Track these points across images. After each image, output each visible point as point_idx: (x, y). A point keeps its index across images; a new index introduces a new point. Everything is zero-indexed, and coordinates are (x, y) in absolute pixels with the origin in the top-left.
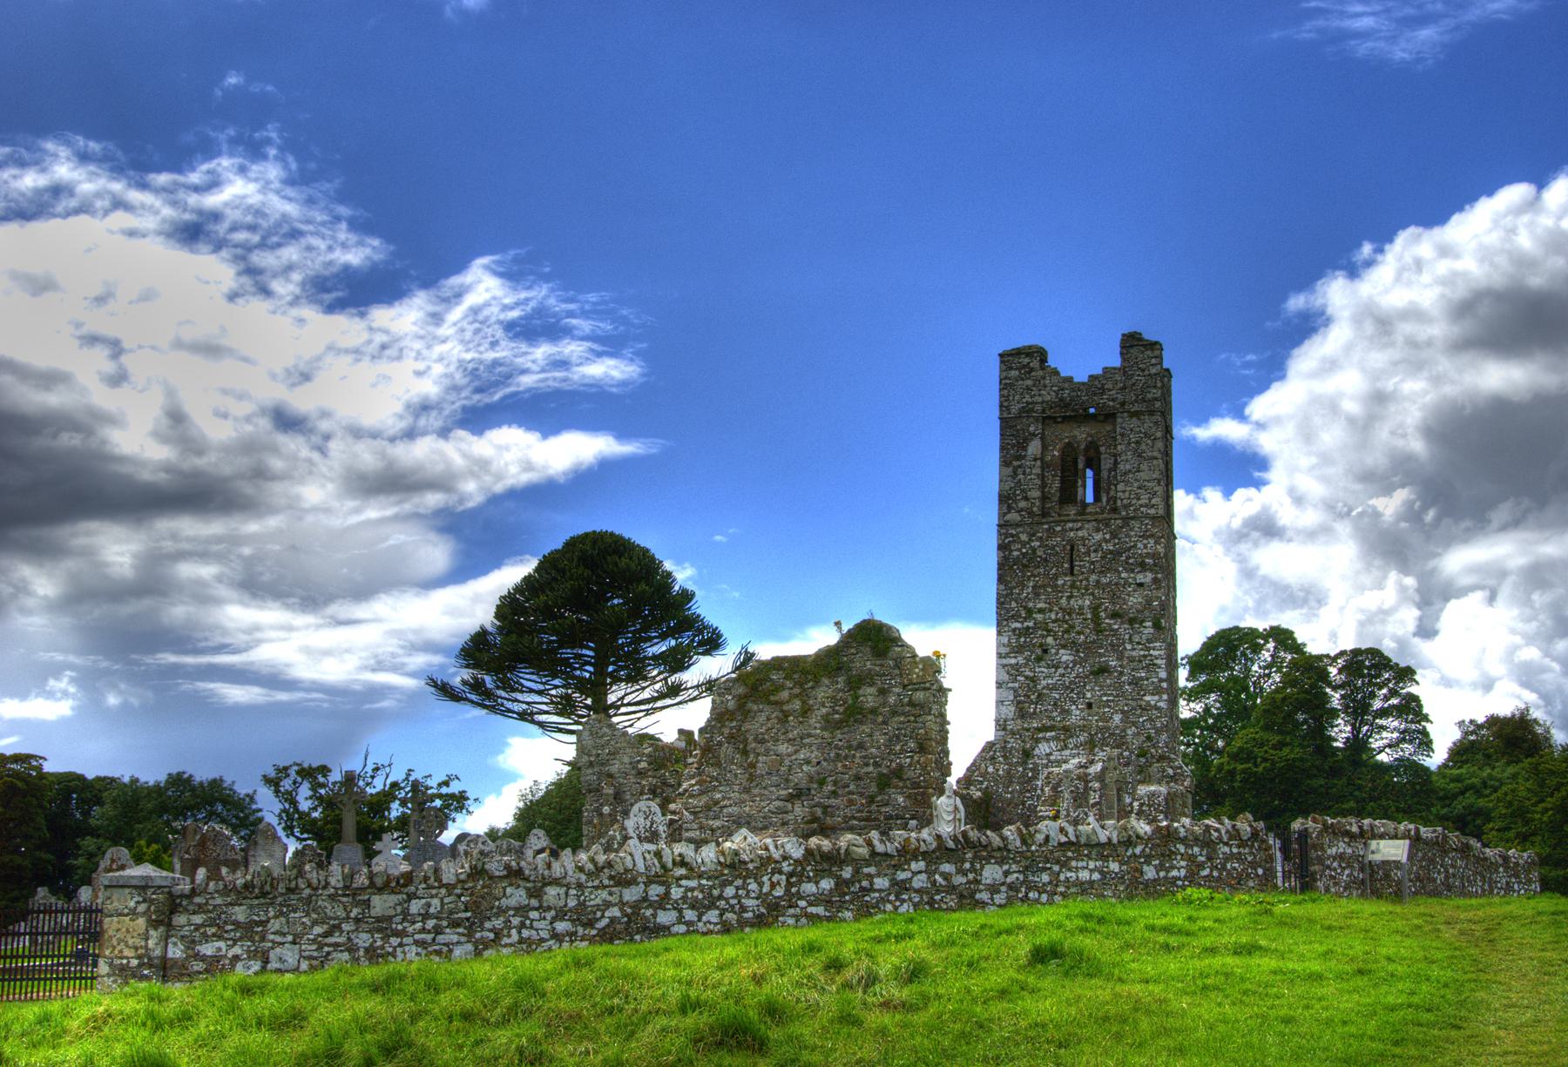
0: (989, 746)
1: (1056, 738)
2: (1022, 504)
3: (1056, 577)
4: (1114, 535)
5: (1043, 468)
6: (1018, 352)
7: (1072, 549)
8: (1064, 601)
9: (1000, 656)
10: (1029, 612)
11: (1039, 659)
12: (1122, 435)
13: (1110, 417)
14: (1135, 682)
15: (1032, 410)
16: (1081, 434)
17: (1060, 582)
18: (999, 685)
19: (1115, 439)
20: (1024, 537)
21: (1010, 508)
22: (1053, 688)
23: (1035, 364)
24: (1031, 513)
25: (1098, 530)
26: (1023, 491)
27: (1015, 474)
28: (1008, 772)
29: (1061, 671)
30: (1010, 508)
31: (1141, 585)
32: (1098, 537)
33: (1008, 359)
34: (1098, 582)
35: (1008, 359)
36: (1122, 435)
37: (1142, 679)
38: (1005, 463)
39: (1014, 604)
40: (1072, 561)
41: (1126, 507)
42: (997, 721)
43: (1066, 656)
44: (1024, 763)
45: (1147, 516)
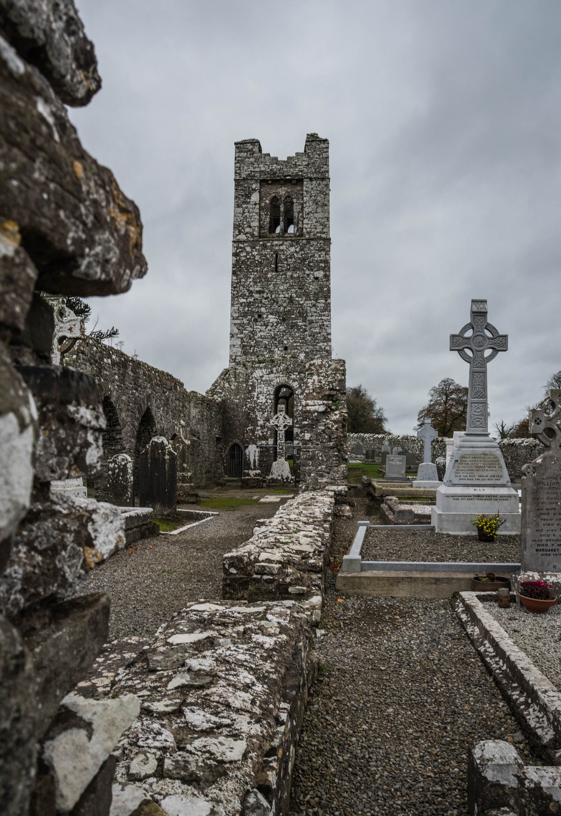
0: (226, 372)
1: (265, 367)
2: (248, 230)
3: (267, 273)
4: (302, 250)
6: (244, 143)
8: (271, 286)
9: (233, 318)
10: (251, 292)
11: (256, 320)
12: (307, 191)
13: (299, 181)
14: (312, 335)
15: (254, 176)
16: (282, 191)
17: (269, 275)
18: (232, 336)
19: (302, 194)
20: (248, 249)
21: (240, 232)
22: (265, 338)
23: (256, 149)
24: (253, 235)
25: (292, 246)
26: (248, 222)
27: (244, 213)
28: (237, 387)
29: (269, 328)
30: (240, 232)
31: (317, 278)
32: (292, 249)
33: (240, 146)
34: (292, 276)
35: (240, 146)
36: (307, 191)
37: (317, 333)
38: (238, 206)
40: (276, 264)
41: (309, 233)
42: (231, 356)
43: (272, 319)
44: (247, 381)
45: (320, 238)
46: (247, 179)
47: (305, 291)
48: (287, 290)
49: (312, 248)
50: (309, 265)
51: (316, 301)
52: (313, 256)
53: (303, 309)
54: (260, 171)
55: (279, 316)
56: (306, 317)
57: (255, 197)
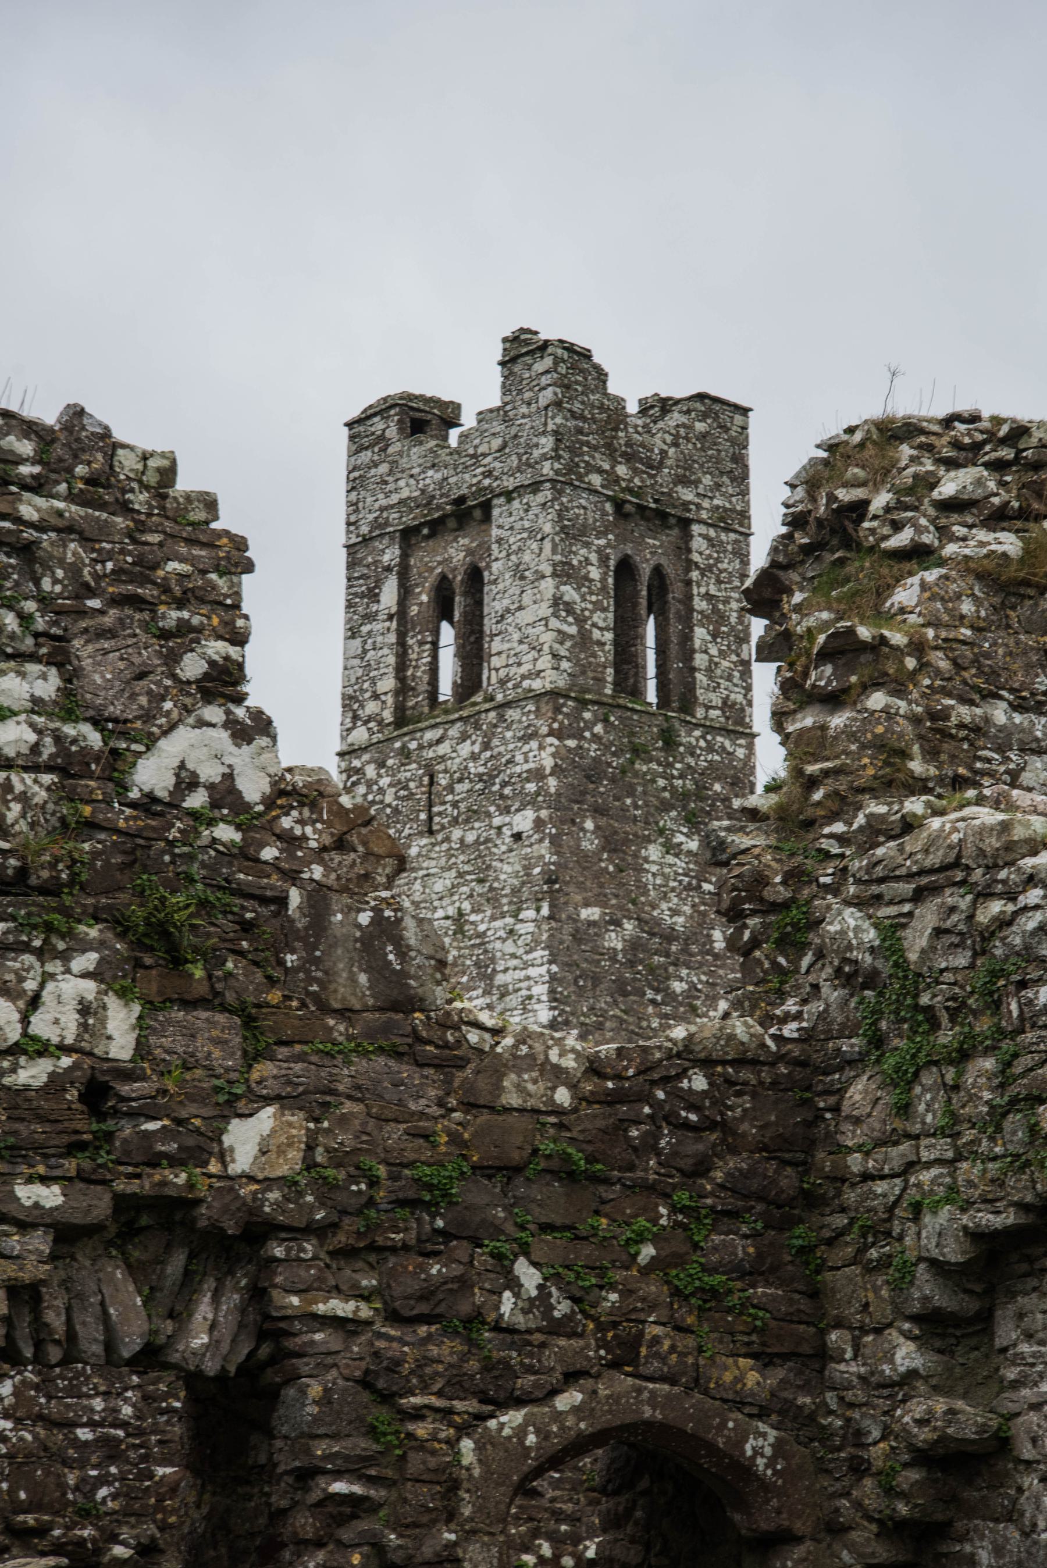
4: (486, 746)
5: (402, 636)
7: (431, 783)
12: (499, 541)
13: (486, 507)
15: (387, 523)
16: (455, 552)
20: (371, 771)
25: (464, 737)
30: (355, 718)
31: (517, 837)
32: (466, 749)
34: (462, 840)
38: (352, 633)
46: (371, 538)
47: (491, 889)
48: (452, 891)
49: (509, 734)
50: (502, 797)
51: (516, 916)
53: (486, 951)
54: (401, 502)
56: (491, 978)
57: (389, 595)
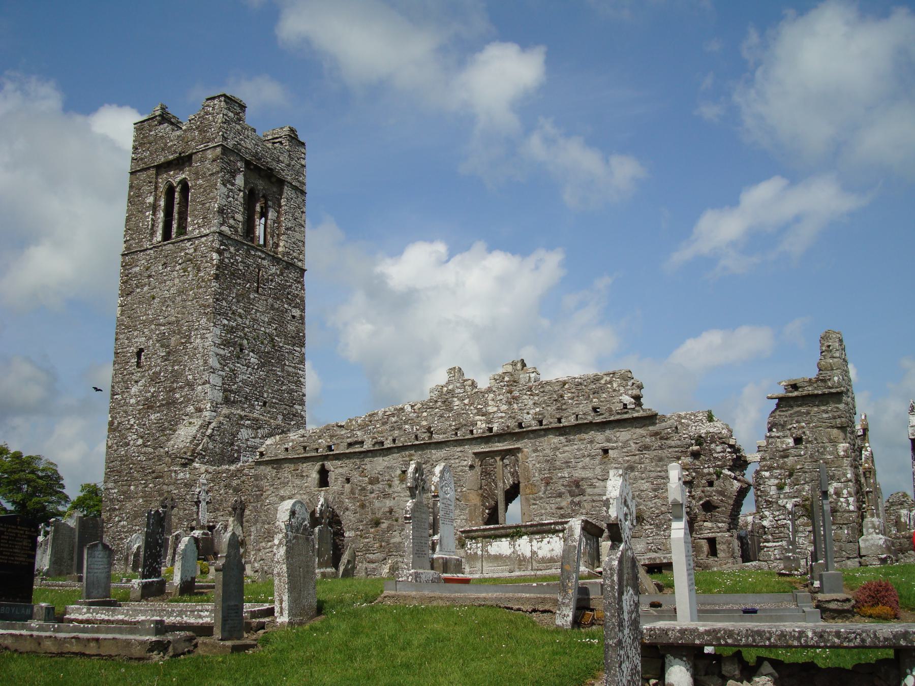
20: (232, 249)
31: (294, 317)
39: (224, 304)
44: (232, 444)
52: (290, 286)
55: (260, 357)
